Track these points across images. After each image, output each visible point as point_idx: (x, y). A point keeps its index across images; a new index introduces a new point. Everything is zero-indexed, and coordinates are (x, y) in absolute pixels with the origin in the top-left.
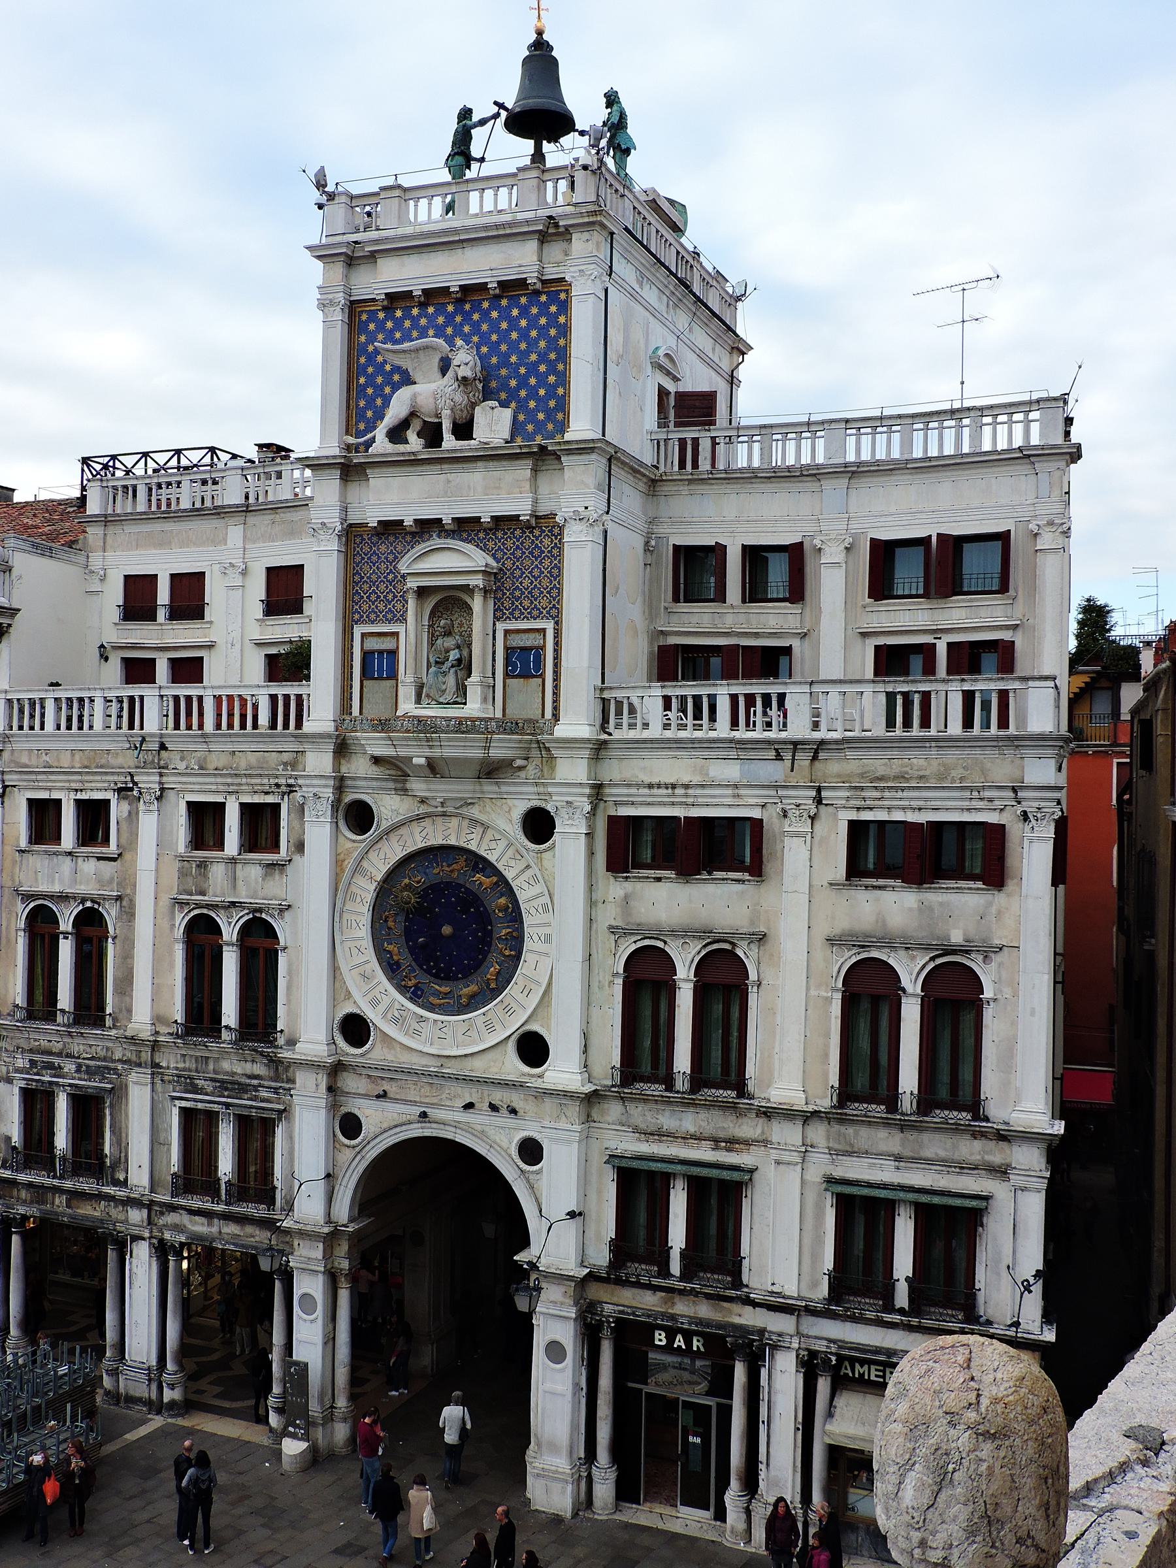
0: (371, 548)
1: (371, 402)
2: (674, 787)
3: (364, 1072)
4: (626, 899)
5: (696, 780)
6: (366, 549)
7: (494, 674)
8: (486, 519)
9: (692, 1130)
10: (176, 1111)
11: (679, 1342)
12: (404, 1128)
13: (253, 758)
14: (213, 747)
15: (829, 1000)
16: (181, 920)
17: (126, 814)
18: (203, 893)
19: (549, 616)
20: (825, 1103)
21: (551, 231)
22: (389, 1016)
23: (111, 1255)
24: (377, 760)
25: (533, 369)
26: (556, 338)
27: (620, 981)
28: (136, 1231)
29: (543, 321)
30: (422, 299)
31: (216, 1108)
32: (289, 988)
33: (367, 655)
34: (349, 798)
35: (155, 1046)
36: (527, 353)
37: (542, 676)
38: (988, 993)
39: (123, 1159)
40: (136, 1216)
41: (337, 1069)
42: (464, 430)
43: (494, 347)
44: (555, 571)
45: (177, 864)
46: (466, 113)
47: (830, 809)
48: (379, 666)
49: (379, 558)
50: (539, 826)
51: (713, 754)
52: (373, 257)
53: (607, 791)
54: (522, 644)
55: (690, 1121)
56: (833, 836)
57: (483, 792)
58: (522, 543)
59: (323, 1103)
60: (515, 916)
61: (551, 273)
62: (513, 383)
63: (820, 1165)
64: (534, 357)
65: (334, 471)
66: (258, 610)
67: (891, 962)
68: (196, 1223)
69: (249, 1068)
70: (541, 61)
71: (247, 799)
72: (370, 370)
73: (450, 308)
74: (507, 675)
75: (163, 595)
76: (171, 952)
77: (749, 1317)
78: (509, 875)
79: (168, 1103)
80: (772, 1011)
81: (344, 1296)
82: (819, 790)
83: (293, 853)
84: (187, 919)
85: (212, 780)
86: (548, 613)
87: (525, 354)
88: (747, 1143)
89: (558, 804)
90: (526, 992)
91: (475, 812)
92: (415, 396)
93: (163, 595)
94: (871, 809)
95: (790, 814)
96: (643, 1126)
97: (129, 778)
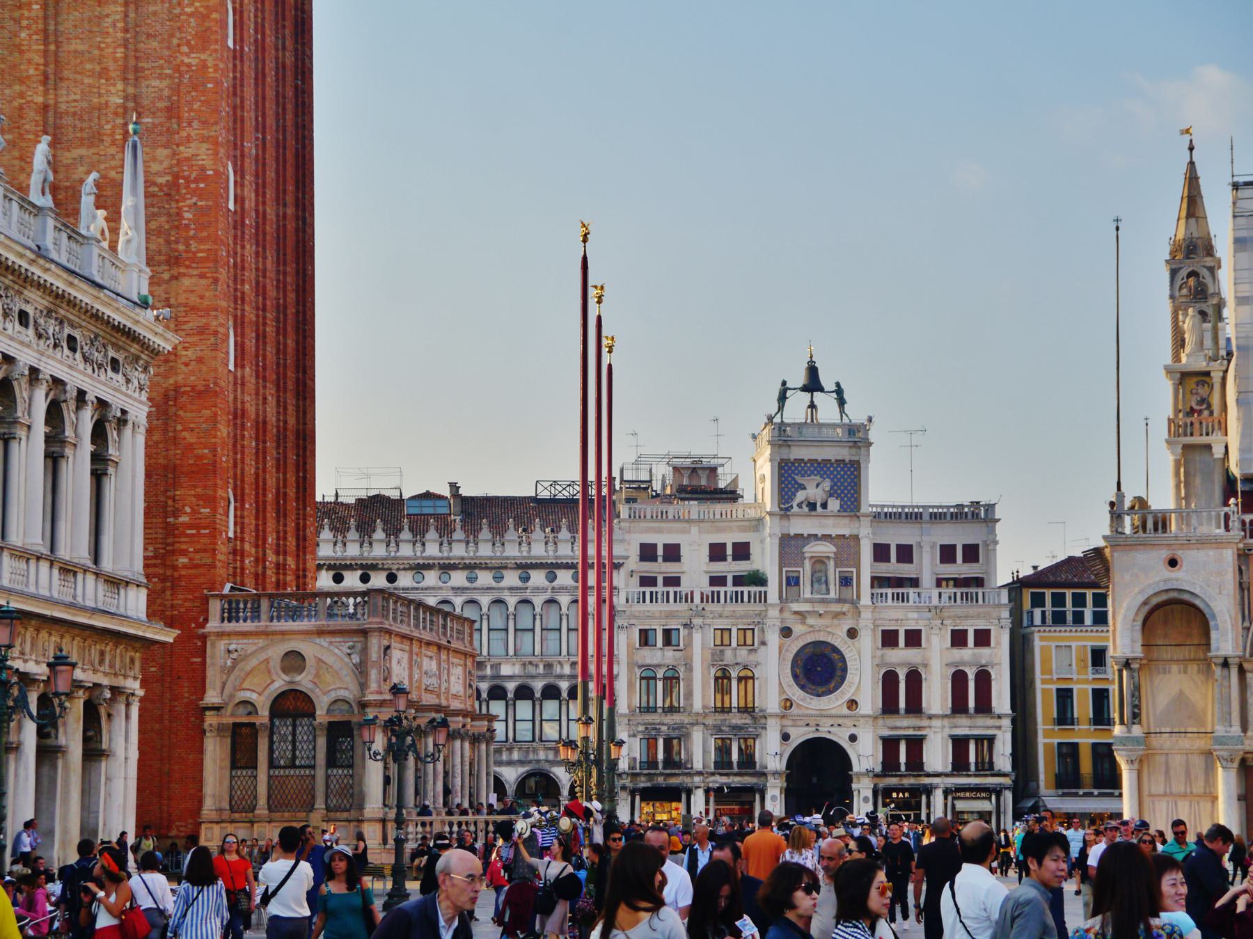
16: (713, 671)
20: (949, 712)
23: (684, 796)
24: (796, 613)
25: (846, 488)
33: (788, 578)
35: (705, 715)
40: (697, 779)
42: (824, 506)
46: (784, 383)
50: (852, 633)
63: (948, 731)
75: (660, 552)
77: (927, 781)
88: (924, 728)
93: (660, 552)
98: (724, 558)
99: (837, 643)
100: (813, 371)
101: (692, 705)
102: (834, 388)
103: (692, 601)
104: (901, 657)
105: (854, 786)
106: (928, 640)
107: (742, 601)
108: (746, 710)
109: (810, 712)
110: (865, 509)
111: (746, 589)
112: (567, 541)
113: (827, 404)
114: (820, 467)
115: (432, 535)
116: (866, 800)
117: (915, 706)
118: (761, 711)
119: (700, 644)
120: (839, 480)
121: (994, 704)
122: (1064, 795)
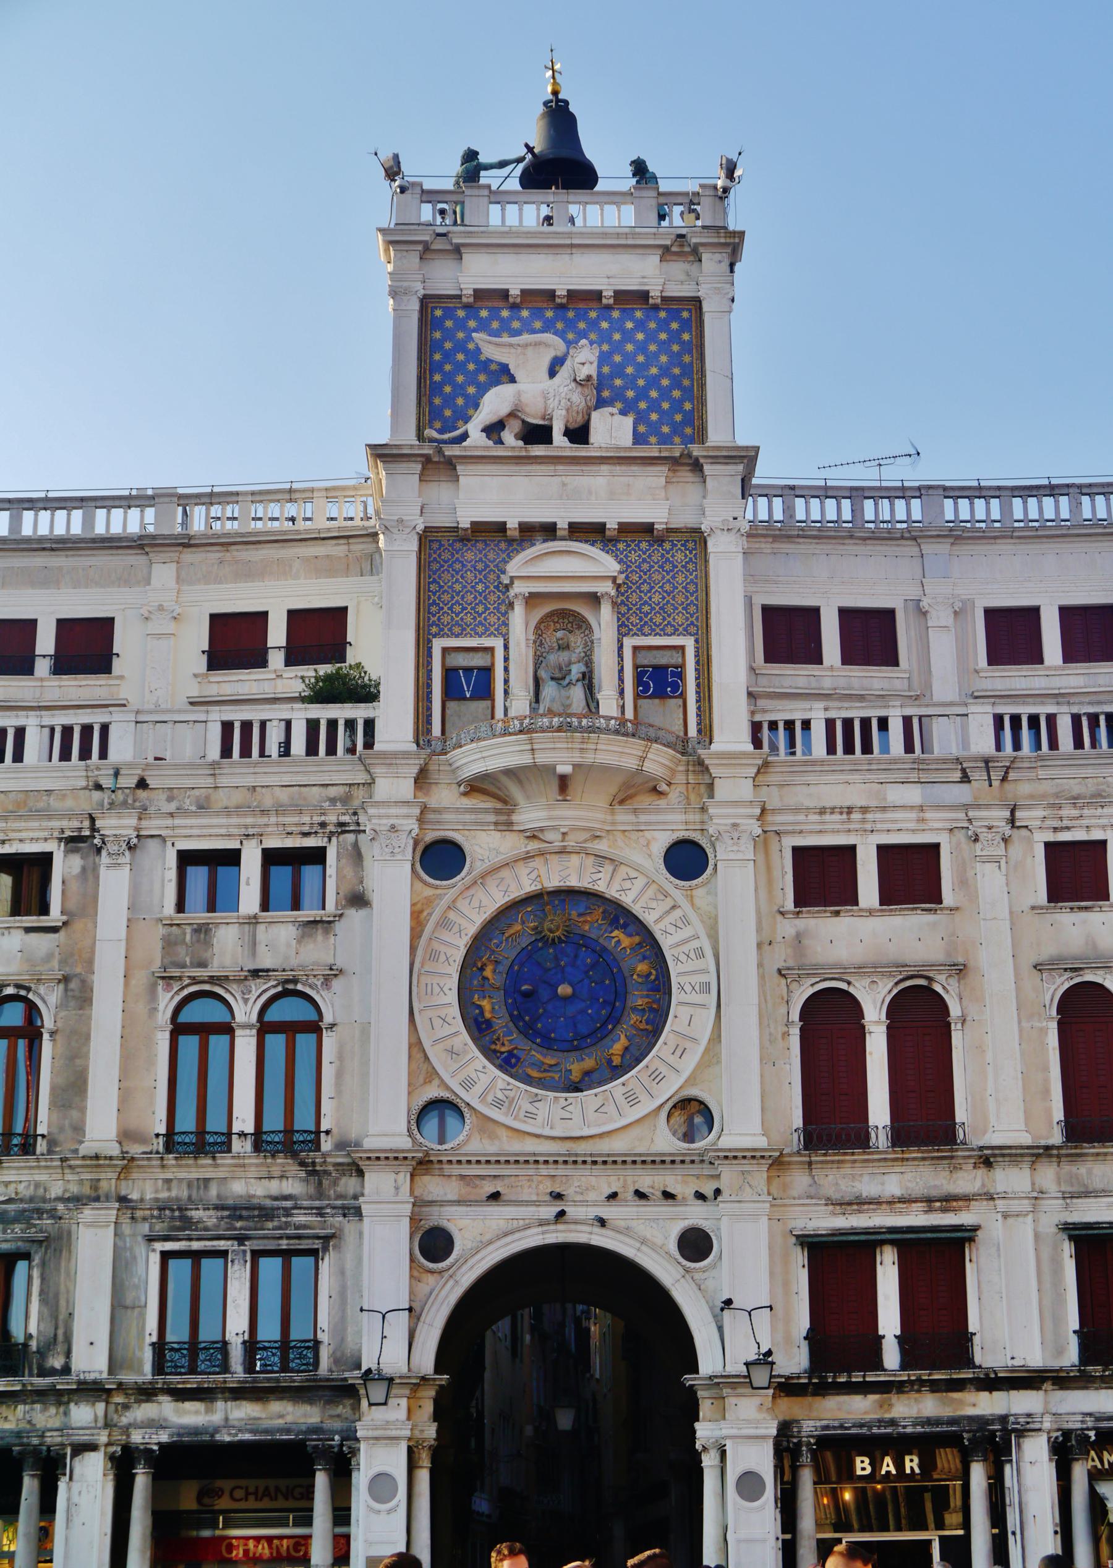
0: (453, 555)
1: (449, 401)
2: (850, 810)
3: (456, 1170)
4: (799, 937)
5: (873, 803)
6: (446, 556)
7: (622, 692)
8: (612, 525)
9: (898, 1192)
10: (155, 1260)
12: (517, 1235)
13: (283, 796)
14: (223, 781)
15: (1044, 1031)
16: (166, 1002)
17: (76, 870)
18: (203, 964)
19: (687, 632)
20: (1056, 1138)
21: (674, 249)
22: (490, 1098)
24: (476, 786)
25: (653, 382)
26: (679, 354)
27: (795, 1032)
28: (83, 1437)
29: (663, 336)
30: (518, 300)
31: (222, 1245)
32: (339, 1075)
33: (449, 674)
34: (430, 837)
35: (127, 1164)
36: (645, 366)
37: (683, 696)
39: (60, 1338)
40: (84, 1415)
42: (579, 434)
43: (603, 359)
44: (692, 588)
45: (161, 931)
46: (471, 156)
47: (1024, 832)
48: (469, 684)
49: (464, 566)
50: (687, 860)
51: (892, 777)
52: (457, 251)
53: (769, 818)
54: (655, 662)
55: (893, 1184)
56: (1029, 860)
57: (613, 823)
58: (650, 556)
59: (408, 1208)
61: (676, 290)
62: (630, 394)
63: (1055, 1213)
64: (654, 371)
65: (413, 465)
66: (201, 663)
68: (189, 1412)
69: (275, 1187)
70: (560, 117)
72: (448, 367)
73: (549, 314)
74: (637, 696)
75: (46, 642)
76: (150, 1042)
78: (649, 918)
79: (141, 1249)
80: (980, 1049)
81: (423, 1477)
82: (1013, 812)
83: (344, 907)
84: (177, 999)
85: (223, 821)
86: (685, 630)
88: (967, 1198)
89: (721, 828)
90: (678, 1053)
91: (602, 846)
92: (519, 393)
93: (46, 642)
94: (1068, 828)
95: (981, 837)
96: (836, 1196)
97: (87, 824)
98: (259, 660)
101: (79, 1129)
103: (103, 755)
104: (869, 942)
105: (704, 1431)
106: (963, 882)
107: (286, 749)
108: (289, 1141)
109: (530, 1146)
110: (716, 436)
111: (300, 715)
116: (749, 1485)
118: (341, 1145)
119: (122, 904)
120: (629, 358)
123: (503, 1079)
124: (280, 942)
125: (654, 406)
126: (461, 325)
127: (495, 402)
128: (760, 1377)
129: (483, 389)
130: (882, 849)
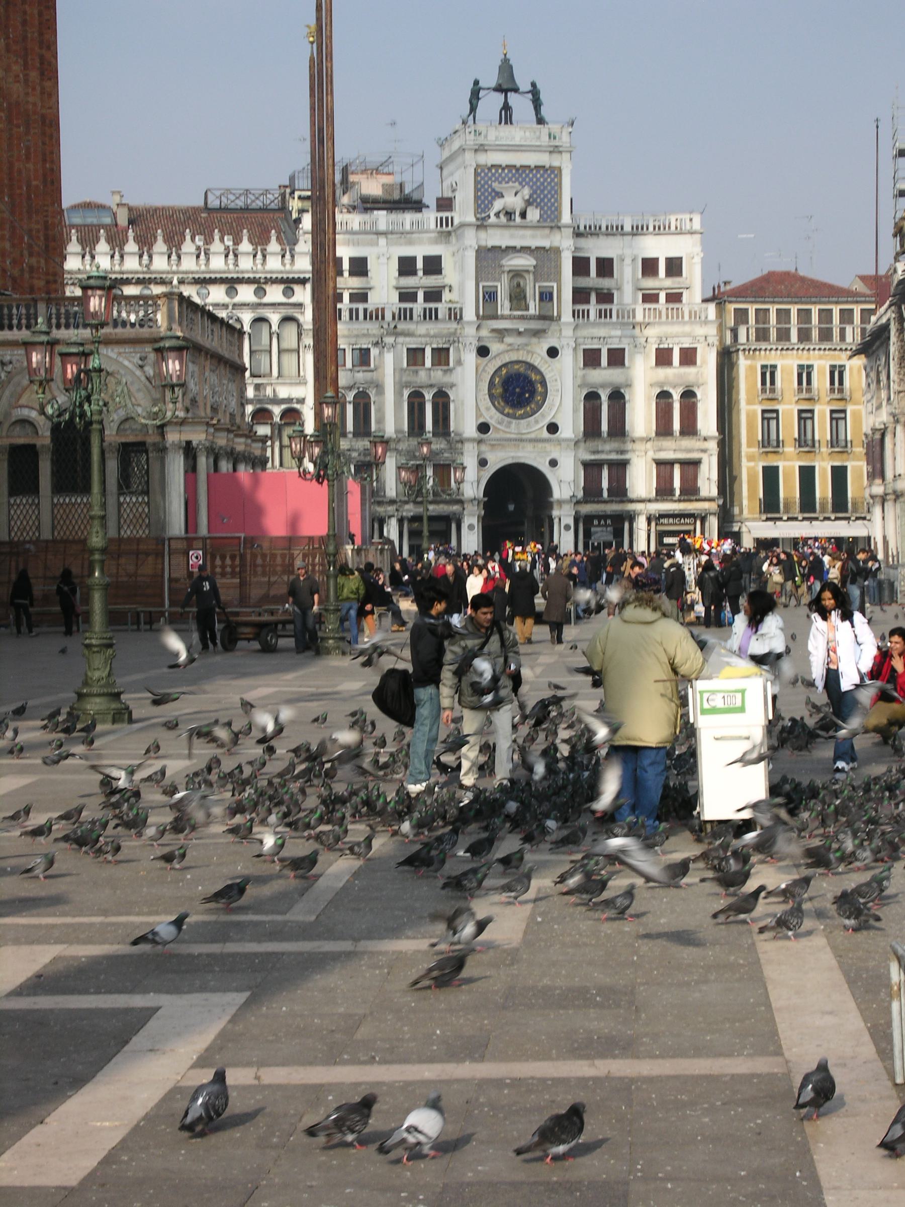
1: (483, 202)
4: (584, 376)
11: (602, 522)
16: (406, 393)
24: (493, 331)
25: (546, 196)
35: (399, 441)
38: (699, 396)
40: (391, 509)
41: (480, 442)
42: (523, 215)
43: (531, 187)
46: (476, 83)
48: (490, 297)
50: (553, 352)
55: (607, 447)
60: (544, 383)
63: (651, 454)
67: (671, 391)
71: (435, 346)
77: (631, 507)
87: (542, 191)
98: (414, 273)
99: (536, 362)
100: (506, 68)
102: (529, 88)
103: (383, 318)
104: (604, 375)
105: (555, 513)
106: (631, 360)
109: (508, 436)
112: (248, 254)
113: (521, 104)
114: (519, 172)
115: (103, 246)
116: (567, 527)
117: (619, 429)
118: (456, 434)
120: (538, 188)
121: (700, 425)
122: (768, 519)
123: (501, 416)
124: (438, 375)
125: (546, 204)
126: (486, 175)
127: (498, 205)
128: (574, 500)
129: (494, 199)
130: (609, 350)
